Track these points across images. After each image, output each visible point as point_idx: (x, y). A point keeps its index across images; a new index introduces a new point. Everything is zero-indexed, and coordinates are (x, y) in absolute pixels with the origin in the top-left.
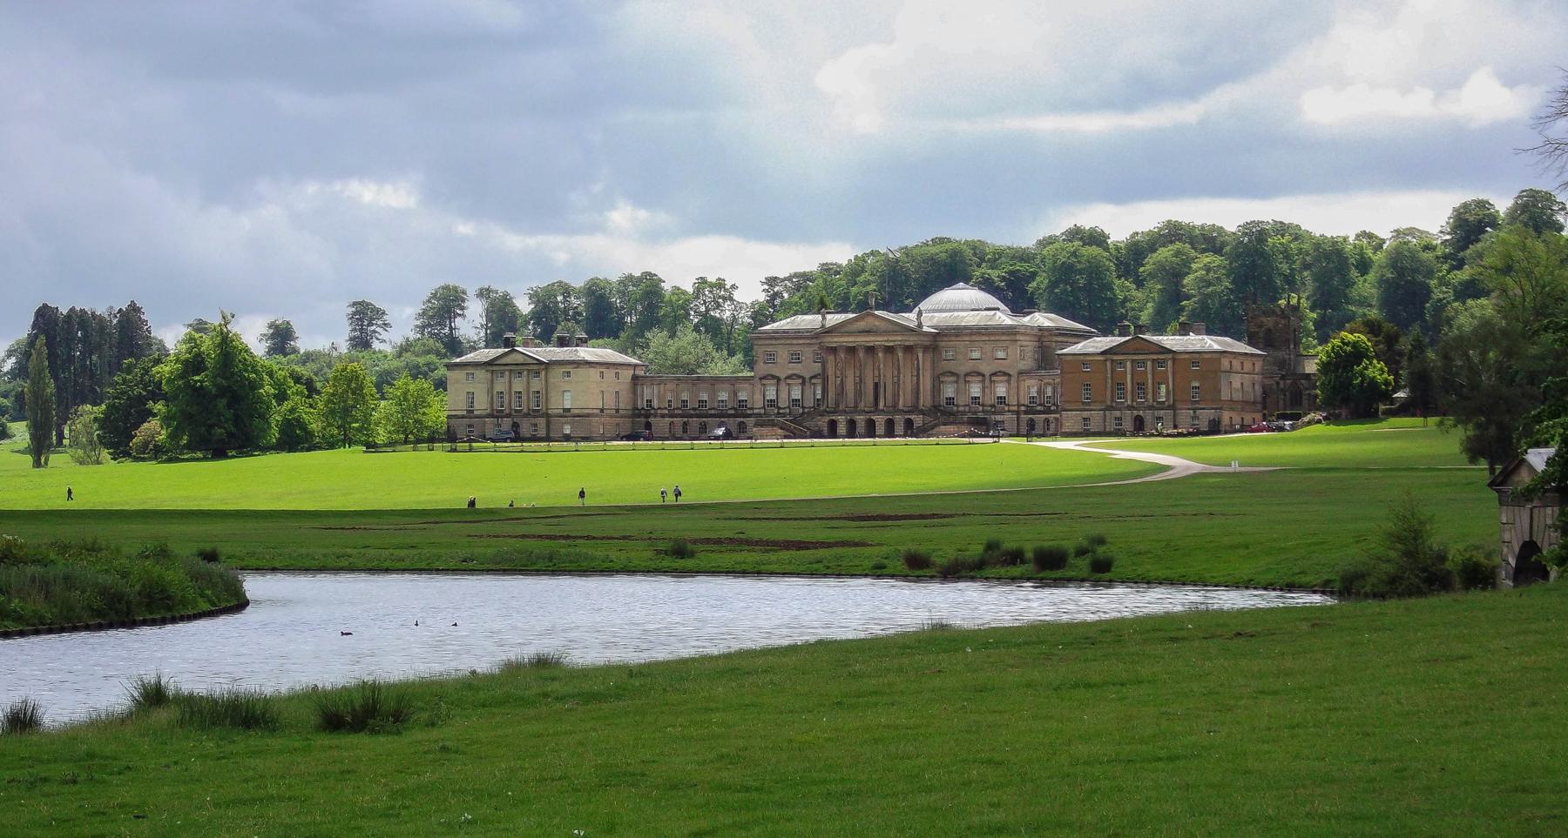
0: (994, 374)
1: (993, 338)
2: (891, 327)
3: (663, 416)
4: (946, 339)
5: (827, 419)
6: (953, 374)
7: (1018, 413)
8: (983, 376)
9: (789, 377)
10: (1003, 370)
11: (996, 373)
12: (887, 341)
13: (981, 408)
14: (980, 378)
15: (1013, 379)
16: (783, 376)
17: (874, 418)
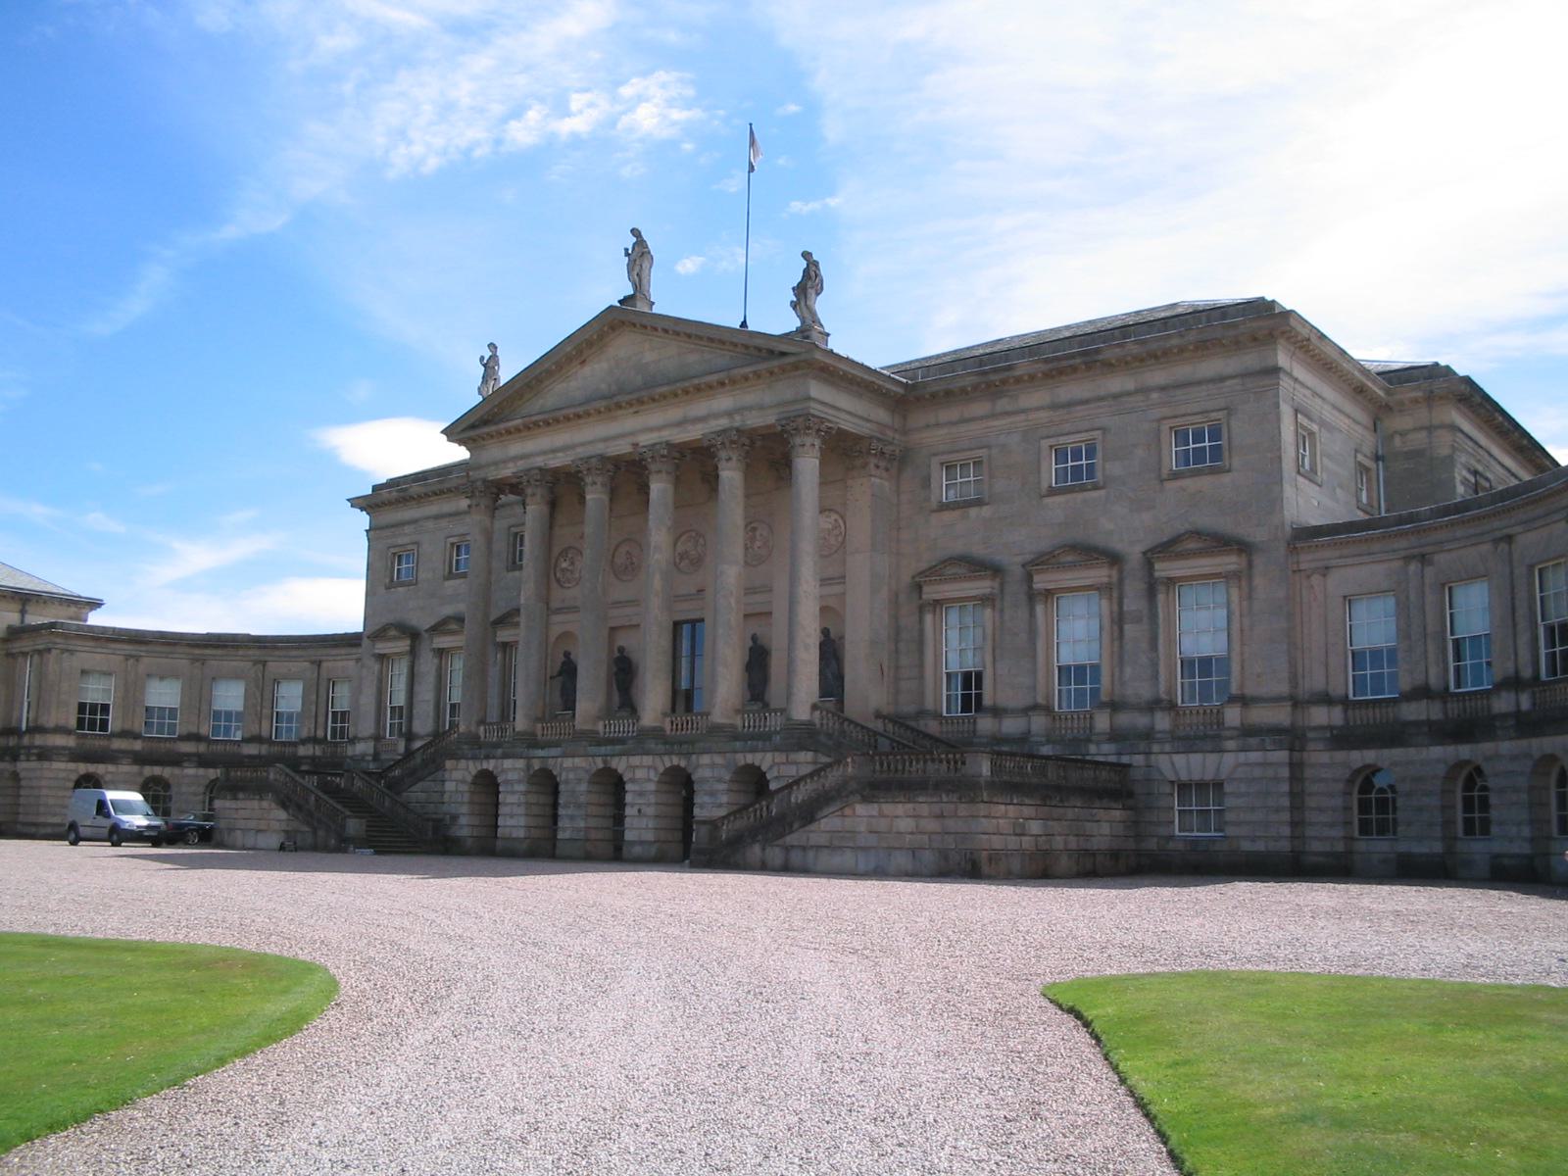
0: (1167, 548)
1: (1157, 376)
2: (695, 359)
3: (45, 754)
5: (474, 767)
6: (978, 566)
7: (1293, 738)
8: (1114, 559)
9: (438, 628)
10: (1206, 520)
11: (1176, 540)
12: (680, 424)
14: (1100, 574)
15: (1259, 561)
16: (423, 621)
17: (620, 764)
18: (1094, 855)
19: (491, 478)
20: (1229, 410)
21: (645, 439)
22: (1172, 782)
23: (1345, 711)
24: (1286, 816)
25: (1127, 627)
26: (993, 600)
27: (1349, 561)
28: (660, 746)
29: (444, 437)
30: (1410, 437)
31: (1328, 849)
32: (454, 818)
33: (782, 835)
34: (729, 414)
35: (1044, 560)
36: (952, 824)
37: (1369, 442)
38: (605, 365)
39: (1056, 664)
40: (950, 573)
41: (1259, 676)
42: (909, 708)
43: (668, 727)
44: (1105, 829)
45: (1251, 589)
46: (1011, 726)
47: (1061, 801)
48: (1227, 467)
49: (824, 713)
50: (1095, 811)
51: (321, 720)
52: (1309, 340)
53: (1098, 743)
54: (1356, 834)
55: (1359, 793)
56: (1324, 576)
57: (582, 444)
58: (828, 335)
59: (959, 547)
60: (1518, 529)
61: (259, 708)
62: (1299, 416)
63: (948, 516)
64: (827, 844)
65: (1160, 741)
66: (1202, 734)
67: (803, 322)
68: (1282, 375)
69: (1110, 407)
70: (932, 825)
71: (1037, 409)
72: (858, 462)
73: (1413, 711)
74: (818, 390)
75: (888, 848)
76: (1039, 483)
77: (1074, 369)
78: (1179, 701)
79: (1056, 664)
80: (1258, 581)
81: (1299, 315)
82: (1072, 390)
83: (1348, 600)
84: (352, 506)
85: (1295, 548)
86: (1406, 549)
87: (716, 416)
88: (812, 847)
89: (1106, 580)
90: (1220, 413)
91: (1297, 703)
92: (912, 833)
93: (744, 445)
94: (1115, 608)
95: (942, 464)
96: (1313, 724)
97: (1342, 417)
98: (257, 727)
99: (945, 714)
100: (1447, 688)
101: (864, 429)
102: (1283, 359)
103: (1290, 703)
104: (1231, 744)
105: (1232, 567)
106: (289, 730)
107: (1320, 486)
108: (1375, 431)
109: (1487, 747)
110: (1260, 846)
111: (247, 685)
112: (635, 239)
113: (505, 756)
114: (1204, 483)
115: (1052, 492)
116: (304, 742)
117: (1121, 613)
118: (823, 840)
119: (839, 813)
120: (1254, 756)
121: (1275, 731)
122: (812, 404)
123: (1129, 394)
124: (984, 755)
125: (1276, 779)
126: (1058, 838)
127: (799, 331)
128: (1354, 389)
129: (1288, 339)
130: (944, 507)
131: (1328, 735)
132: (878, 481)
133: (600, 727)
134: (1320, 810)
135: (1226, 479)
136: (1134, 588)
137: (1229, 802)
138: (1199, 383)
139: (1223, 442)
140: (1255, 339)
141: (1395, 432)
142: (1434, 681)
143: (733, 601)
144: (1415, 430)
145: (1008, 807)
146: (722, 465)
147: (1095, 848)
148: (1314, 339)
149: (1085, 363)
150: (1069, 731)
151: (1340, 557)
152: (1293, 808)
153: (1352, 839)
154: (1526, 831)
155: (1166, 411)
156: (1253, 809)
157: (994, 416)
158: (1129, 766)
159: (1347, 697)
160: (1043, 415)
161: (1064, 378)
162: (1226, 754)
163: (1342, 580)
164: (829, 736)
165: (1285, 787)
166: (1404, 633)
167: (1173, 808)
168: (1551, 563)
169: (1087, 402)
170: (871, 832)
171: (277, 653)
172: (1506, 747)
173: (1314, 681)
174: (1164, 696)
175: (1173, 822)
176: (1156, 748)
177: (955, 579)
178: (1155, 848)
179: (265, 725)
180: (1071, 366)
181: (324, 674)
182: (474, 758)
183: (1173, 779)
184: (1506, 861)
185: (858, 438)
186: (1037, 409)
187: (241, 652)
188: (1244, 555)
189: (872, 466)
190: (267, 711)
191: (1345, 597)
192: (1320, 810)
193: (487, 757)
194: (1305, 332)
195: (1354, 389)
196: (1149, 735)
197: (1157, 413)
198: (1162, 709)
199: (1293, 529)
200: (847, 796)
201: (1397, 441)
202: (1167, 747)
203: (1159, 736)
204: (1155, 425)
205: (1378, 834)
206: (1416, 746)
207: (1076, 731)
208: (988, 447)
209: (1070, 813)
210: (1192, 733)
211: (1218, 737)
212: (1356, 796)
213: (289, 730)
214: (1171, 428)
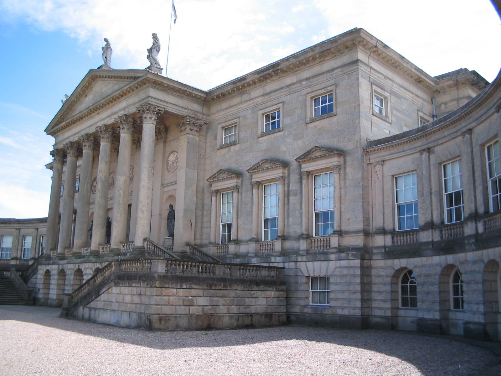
0: (306, 157)
1: (306, 74)
4: (225, 105)
8: (285, 165)
13: (278, 246)
15: (348, 159)
17: (82, 267)
18: (252, 316)
19: (59, 148)
20: (336, 85)
21: (100, 124)
22: (308, 277)
23: (393, 238)
24: (359, 296)
25: (291, 198)
26: (238, 189)
27: (394, 156)
28: (94, 259)
29: (45, 133)
30: (448, 105)
31: (383, 315)
32: (39, 290)
33: (89, 303)
34: (124, 109)
35: (256, 168)
36: (145, 300)
37: (428, 108)
38: (92, 96)
39: (263, 218)
40: (222, 177)
41: (349, 219)
42: (198, 242)
43: (101, 250)
44: (262, 302)
45: (345, 174)
46: (243, 249)
47: (224, 287)
48: (335, 113)
49: (148, 242)
50: (254, 292)
51: (37, 251)
52: (376, 47)
53: (275, 257)
54: (400, 306)
55: (402, 283)
56: (382, 165)
57: (83, 130)
58: (162, 69)
59: (225, 166)
60: (474, 124)
61: (17, 246)
62: (373, 85)
63: (223, 151)
64: (103, 308)
65: (302, 256)
66: (322, 251)
67: (151, 63)
68: (359, 64)
69: (286, 91)
70: (137, 299)
71: (257, 97)
72: (183, 128)
73: (425, 237)
74: (153, 93)
75: (122, 311)
76: (257, 131)
77: (271, 76)
78: (314, 235)
79: (263, 218)
80: (349, 170)
81: (429, 76)
82: (271, 86)
83: (395, 178)
84: (47, 168)
85: (368, 152)
86: (420, 146)
87: (120, 110)
88: (98, 308)
89: (281, 175)
90: (332, 87)
91: (367, 234)
92: (130, 303)
93: (130, 122)
94: (286, 189)
95: (223, 128)
96: (376, 246)
97: (408, 93)
98: (16, 253)
99: (220, 244)
100: (443, 223)
101: (184, 113)
102: (361, 55)
103: (363, 234)
104: (332, 257)
105: (336, 163)
106: (6, 254)
107: (391, 124)
108: (432, 103)
109: (461, 256)
110: (346, 312)
111: (13, 238)
112: (106, 43)
113: (53, 264)
114: (325, 123)
115: (263, 135)
116: (13, 259)
117: (288, 192)
118: (101, 307)
119: (107, 291)
120: (344, 263)
121: (356, 249)
122: (150, 99)
123: (293, 84)
124: (160, 261)
125: (354, 276)
126: (222, 307)
127: (149, 68)
128: (416, 80)
129: (364, 46)
130: (222, 147)
131: (383, 251)
132: (191, 136)
133: (82, 251)
134: (379, 292)
135: (334, 119)
136: (294, 177)
137: (332, 287)
138: (323, 74)
139: (334, 102)
140: (347, 47)
141: (442, 103)
142: (436, 219)
143: (121, 192)
144: (451, 101)
145: (178, 290)
146: (121, 131)
147: (253, 312)
148: (380, 46)
149: (274, 71)
150: (266, 251)
151: (390, 154)
152: (362, 291)
153: (398, 308)
154: (482, 308)
155: (309, 90)
156: (343, 292)
157: (241, 103)
158: (284, 268)
159: (394, 230)
160: (260, 100)
161: (268, 81)
162: (331, 262)
163: (392, 167)
164: (149, 253)
165: (358, 280)
166: (421, 194)
167: (308, 291)
168: (492, 142)
169: (276, 91)
170: (117, 302)
171: (24, 225)
172: (471, 255)
173: (377, 222)
174: (304, 232)
175: (308, 298)
176: (299, 259)
177: (224, 179)
178: (299, 311)
179: (19, 252)
180: (268, 74)
181: (39, 234)
182: (45, 265)
183: (308, 275)
184: (472, 326)
185: (183, 117)
186: (257, 97)
187: (12, 225)
188: (342, 157)
189: (188, 129)
190: (20, 248)
191: (393, 176)
192: (379, 292)
193: (49, 264)
194: (374, 42)
195: (416, 80)
196: (296, 253)
197: (304, 92)
198: (303, 239)
199: (368, 142)
200: (110, 283)
201: (443, 107)
202: (304, 259)
203: (301, 252)
204: (305, 97)
205: (411, 307)
206: (426, 256)
207: (269, 251)
208: (239, 117)
209: (232, 294)
210: (317, 251)
211: (328, 253)
212: (400, 285)
213: (6, 254)
214: (312, 98)
